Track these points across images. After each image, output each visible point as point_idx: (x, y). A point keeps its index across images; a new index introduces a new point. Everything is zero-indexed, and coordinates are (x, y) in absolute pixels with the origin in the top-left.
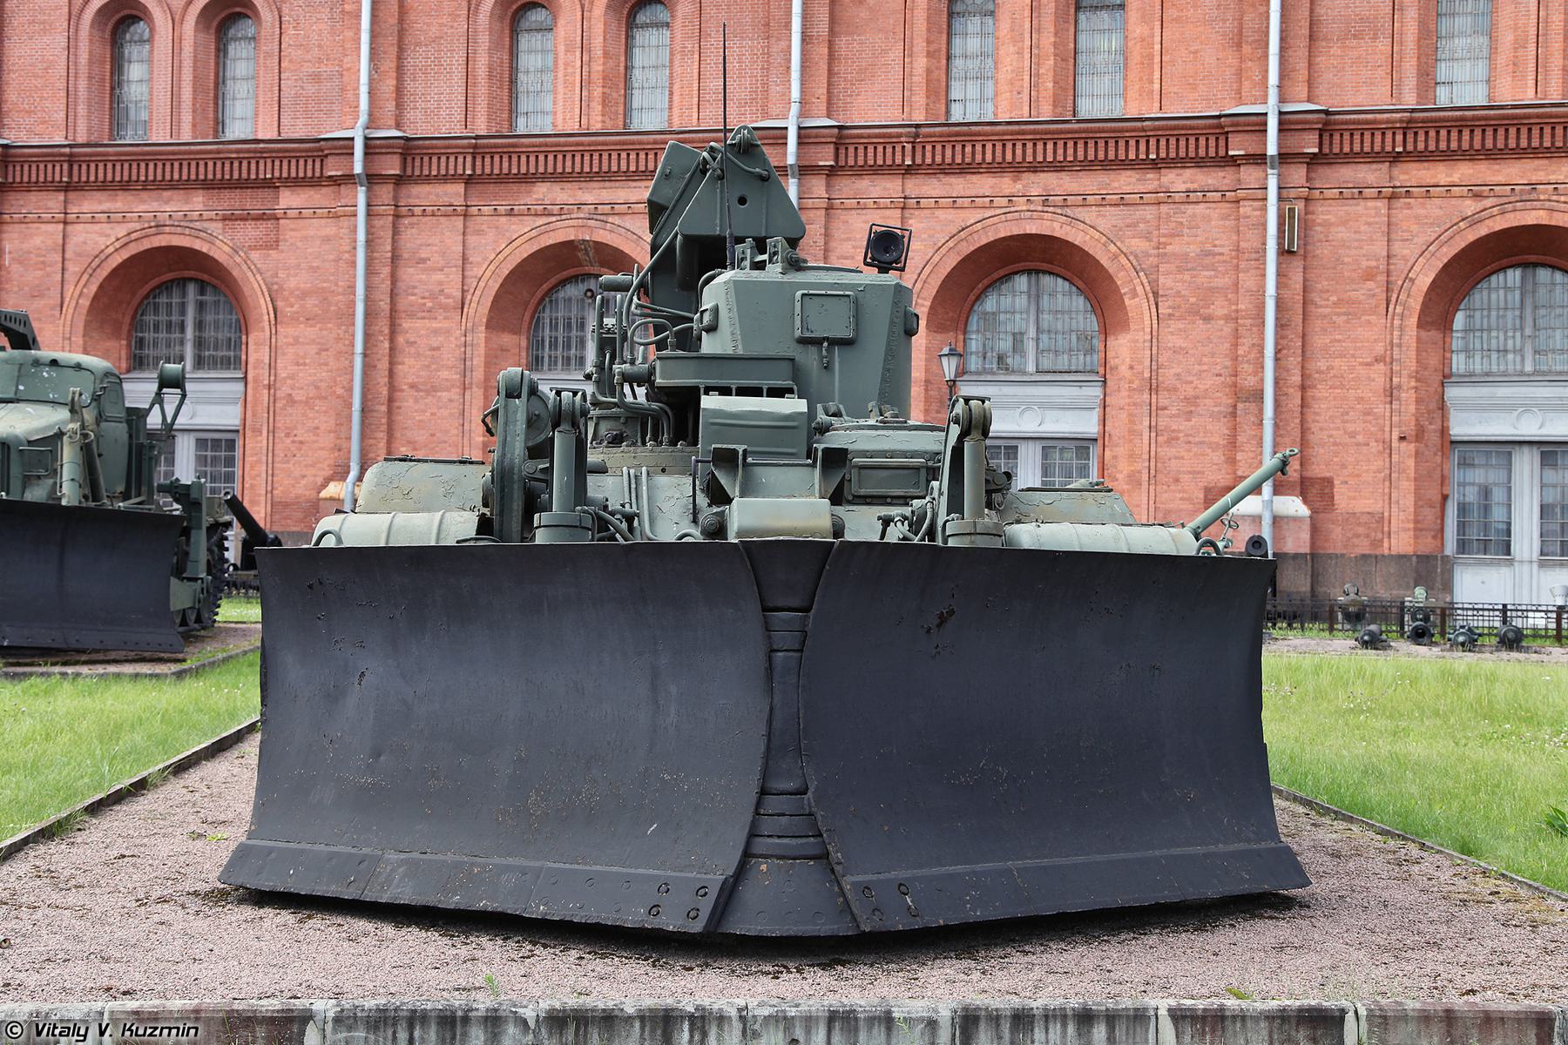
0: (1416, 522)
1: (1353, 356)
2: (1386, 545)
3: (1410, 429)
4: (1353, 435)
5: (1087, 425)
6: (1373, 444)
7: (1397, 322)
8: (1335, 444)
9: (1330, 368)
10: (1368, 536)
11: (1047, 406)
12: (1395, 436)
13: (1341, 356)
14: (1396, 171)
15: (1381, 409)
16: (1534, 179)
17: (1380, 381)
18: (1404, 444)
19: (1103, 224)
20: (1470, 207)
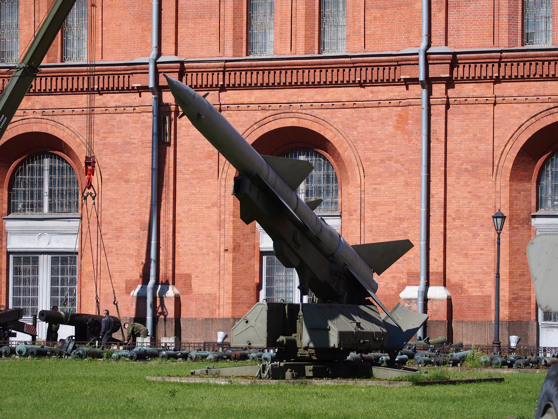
0: (234, 298)
1: (201, 203)
2: (217, 312)
3: (230, 246)
4: (201, 249)
5: (69, 243)
6: (211, 254)
7: (223, 183)
8: (192, 254)
9: (190, 210)
10: (209, 307)
11: (52, 232)
12: (222, 249)
13: (195, 203)
14: (223, 94)
15: (216, 234)
16: (291, 100)
17: (215, 218)
18: (227, 254)
19: (74, 126)
20: (260, 115)
